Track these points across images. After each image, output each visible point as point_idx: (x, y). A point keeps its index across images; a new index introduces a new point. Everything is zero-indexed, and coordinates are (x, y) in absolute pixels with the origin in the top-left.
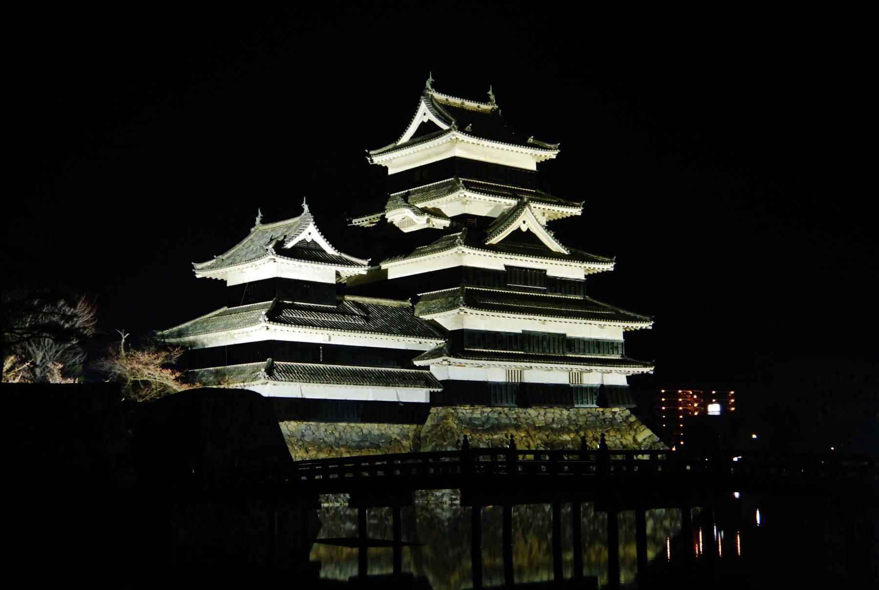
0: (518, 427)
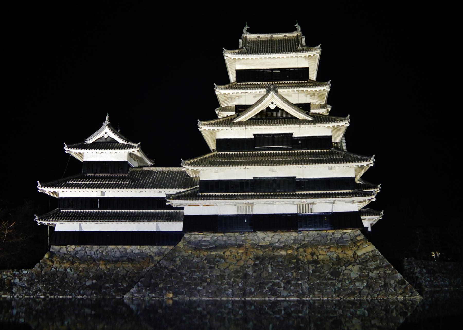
0: (240, 246)
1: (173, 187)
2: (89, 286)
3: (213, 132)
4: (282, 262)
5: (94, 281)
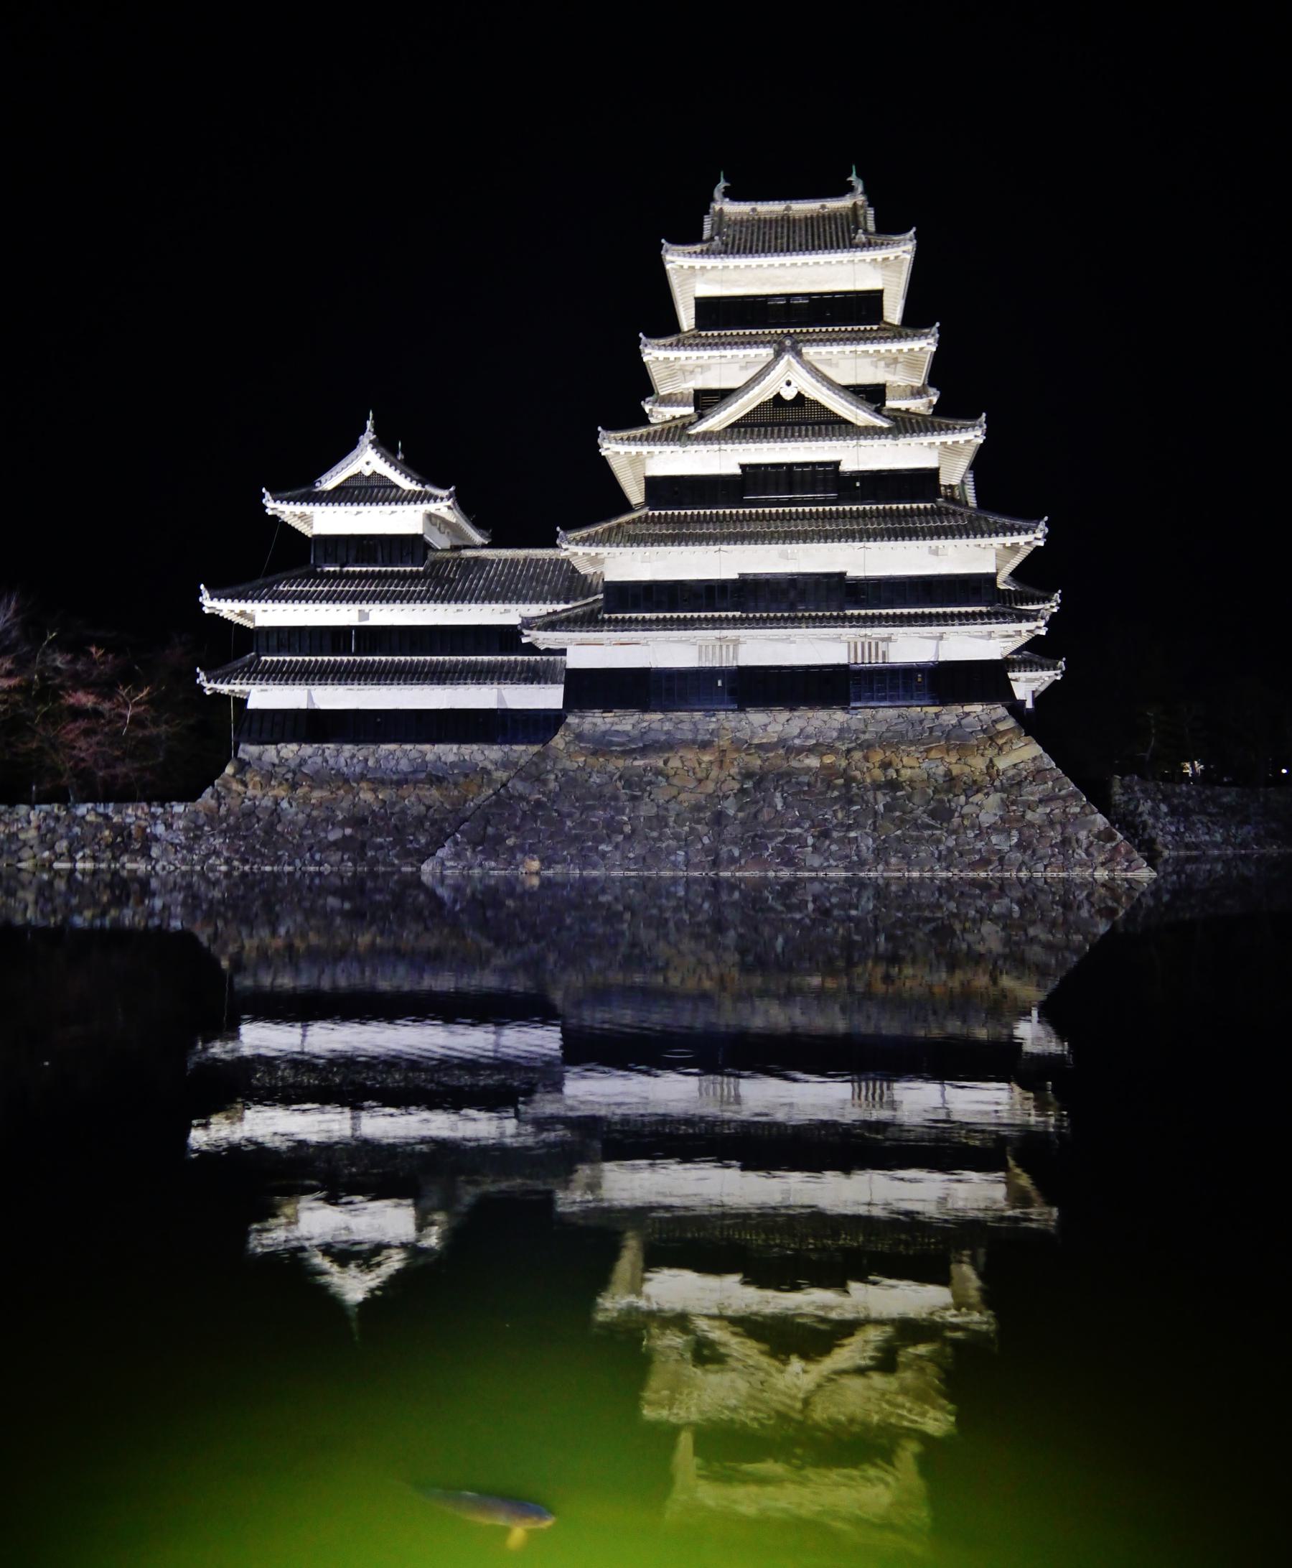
0: (705, 745)
1: (537, 599)
2: (335, 843)
3: (638, 460)
4: (809, 785)
5: (348, 831)
